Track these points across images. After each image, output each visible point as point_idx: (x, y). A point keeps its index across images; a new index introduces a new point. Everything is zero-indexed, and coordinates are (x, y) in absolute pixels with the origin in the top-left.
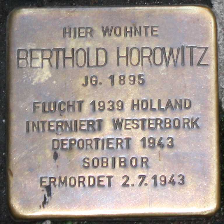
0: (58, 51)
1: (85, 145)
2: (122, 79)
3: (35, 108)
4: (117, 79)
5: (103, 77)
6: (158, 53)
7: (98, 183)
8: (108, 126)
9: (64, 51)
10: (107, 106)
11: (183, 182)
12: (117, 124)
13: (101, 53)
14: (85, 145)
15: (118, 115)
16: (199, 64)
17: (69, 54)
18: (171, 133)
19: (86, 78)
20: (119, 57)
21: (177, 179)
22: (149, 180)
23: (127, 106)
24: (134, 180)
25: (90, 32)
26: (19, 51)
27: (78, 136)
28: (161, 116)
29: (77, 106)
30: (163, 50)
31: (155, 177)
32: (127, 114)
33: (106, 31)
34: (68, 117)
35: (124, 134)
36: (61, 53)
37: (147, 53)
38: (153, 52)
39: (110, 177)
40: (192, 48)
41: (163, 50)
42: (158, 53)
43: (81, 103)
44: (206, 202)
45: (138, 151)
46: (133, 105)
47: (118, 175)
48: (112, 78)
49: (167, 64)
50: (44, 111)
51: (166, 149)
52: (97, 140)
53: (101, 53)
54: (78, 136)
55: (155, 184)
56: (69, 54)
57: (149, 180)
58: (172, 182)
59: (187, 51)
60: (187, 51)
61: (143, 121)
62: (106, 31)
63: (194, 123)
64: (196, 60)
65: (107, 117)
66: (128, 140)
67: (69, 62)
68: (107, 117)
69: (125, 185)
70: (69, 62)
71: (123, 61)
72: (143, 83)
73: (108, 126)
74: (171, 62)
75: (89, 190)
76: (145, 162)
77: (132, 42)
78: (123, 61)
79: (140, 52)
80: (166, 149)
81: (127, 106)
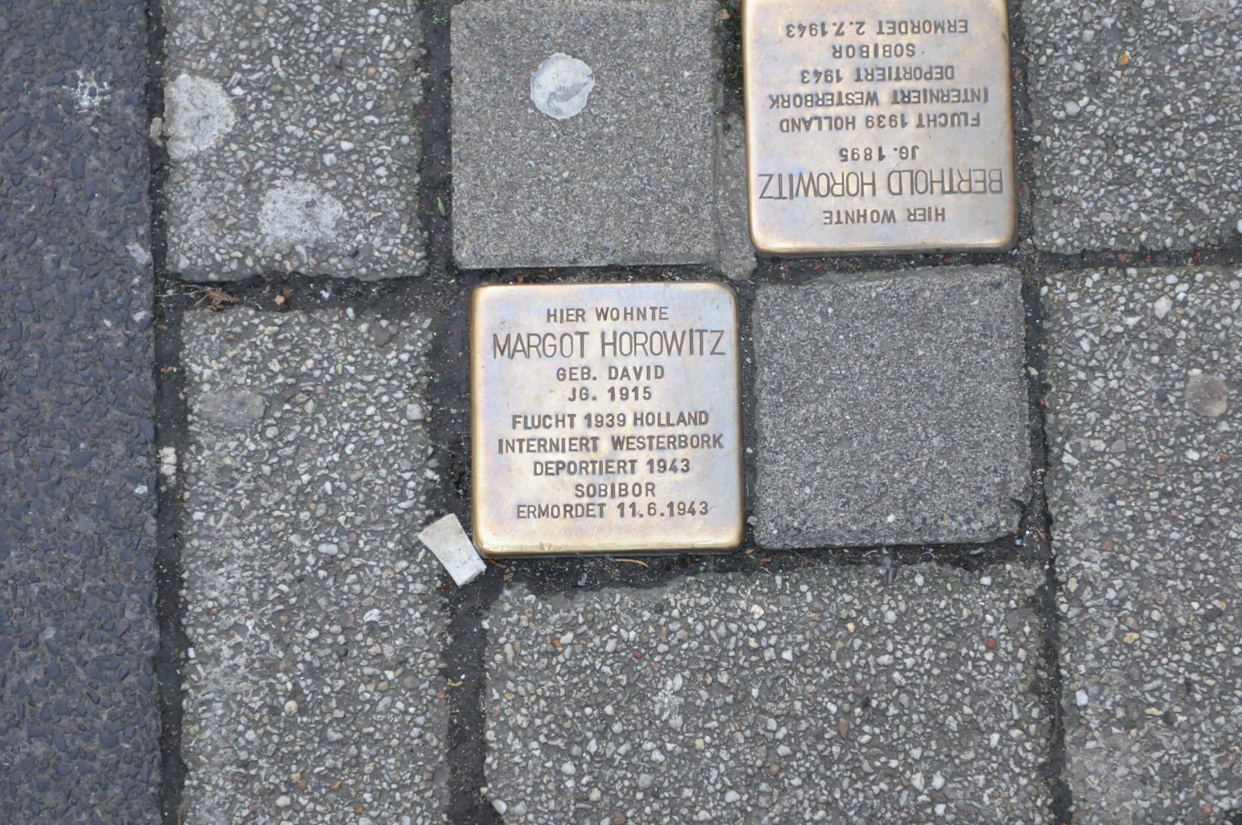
0: (951, 191)
1: (912, 74)
2: (868, 157)
3: (978, 119)
4: (875, 155)
5: (892, 161)
6: (823, 191)
7: (895, 27)
8: (884, 97)
9: (943, 192)
10: (886, 122)
11: (789, 28)
12: (872, 98)
13: (895, 189)
14: (912, 74)
15: (872, 110)
16: (771, 176)
17: (937, 187)
18: (804, 90)
19: (914, 157)
20: (873, 184)
21: (796, 31)
22: (832, 30)
23: (860, 122)
24: (849, 30)
25: (911, 216)
26: (1001, 191)
27: (922, 84)
28: (820, 111)
29: (925, 122)
30: (817, 193)
31: (824, 33)
32: (861, 113)
33: (890, 217)
34: (936, 108)
35: (865, 87)
36: (947, 188)
37: (838, 190)
38: (830, 189)
39: (881, 32)
40: (781, 197)
41: (817, 193)
42: (823, 191)
43: (920, 125)
45: (845, 67)
46: (853, 123)
47: (870, 36)
48: (881, 157)
49: (669, 350)
50: (966, 114)
51: (811, 69)
52: (898, 79)
53: (895, 189)
54: (922, 84)
55: (823, 25)
56: (937, 187)
57: (832, 30)
59: (786, 193)
60: (786, 193)
61: (840, 103)
63: (775, 102)
64: (775, 181)
65: (885, 107)
66: (858, 80)
68: (885, 107)
69: (862, 24)
71: (867, 179)
72: (842, 151)
73: (884, 97)
75: (906, 18)
76: (836, 52)
77: (855, 204)
78: (867, 179)
79: (846, 191)
80: (811, 69)
81: (860, 122)
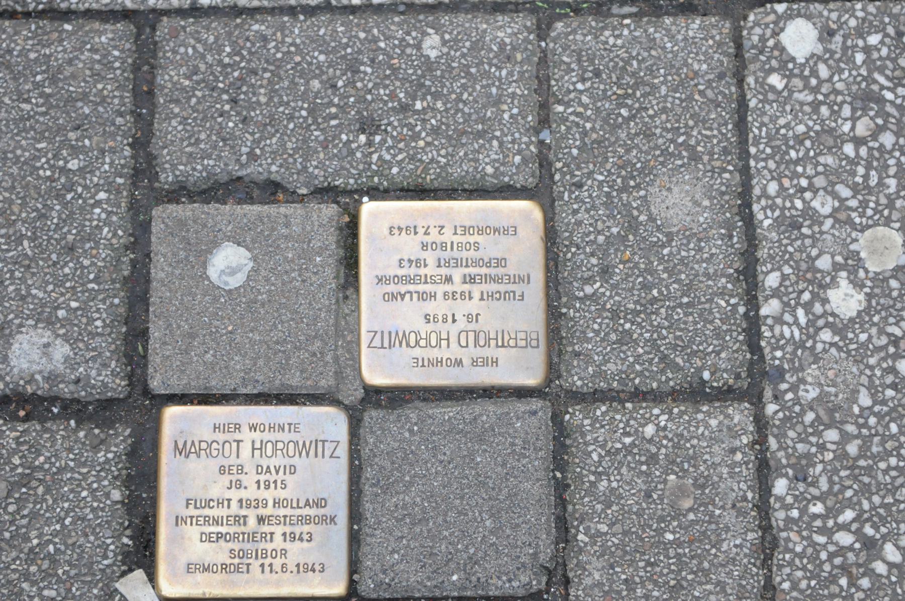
0: (503, 346)
1: (477, 263)
2: (445, 320)
3: (522, 296)
4: (450, 319)
5: (462, 324)
6: (412, 343)
7: (466, 230)
8: (457, 278)
9: (497, 346)
10: (458, 296)
11: (391, 228)
12: (449, 279)
13: (463, 343)
14: (477, 263)
15: (448, 288)
16: (376, 332)
17: (493, 343)
18: (401, 272)
19: (477, 321)
20: (448, 339)
21: (396, 231)
22: (421, 231)
23: (440, 296)
24: (434, 231)
25: (474, 363)
26: (538, 347)
27: (484, 271)
28: (411, 288)
29: (485, 297)
30: (408, 345)
31: (416, 233)
32: (440, 289)
33: (459, 363)
34: (494, 287)
35: (444, 271)
36: (500, 344)
37: (423, 343)
38: (417, 343)
39: (455, 234)
40: (382, 347)
41: (408, 345)
42: (412, 343)
43: (482, 299)
44: (374, 215)
45: (430, 257)
47: (448, 236)
48: (454, 321)
49: (300, 454)
50: (514, 292)
51: (406, 258)
52: (467, 266)
53: (463, 343)
54: (484, 271)
55: (415, 227)
56: (493, 343)
57: (421, 231)
58: (400, 229)
59: (386, 344)
60: (386, 344)
61: (426, 282)
62: (459, 363)
63: (380, 280)
64: (379, 335)
65: (458, 286)
66: (439, 266)
67: (492, 335)
68: (458, 286)
69: (442, 227)
70: (492, 335)
71: (444, 336)
72: (426, 316)
73: (457, 278)
74: (401, 335)
75: (473, 224)
76: (424, 247)
77: (435, 354)
78: (444, 336)
79: (429, 344)
80: (406, 258)
81: (440, 296)
